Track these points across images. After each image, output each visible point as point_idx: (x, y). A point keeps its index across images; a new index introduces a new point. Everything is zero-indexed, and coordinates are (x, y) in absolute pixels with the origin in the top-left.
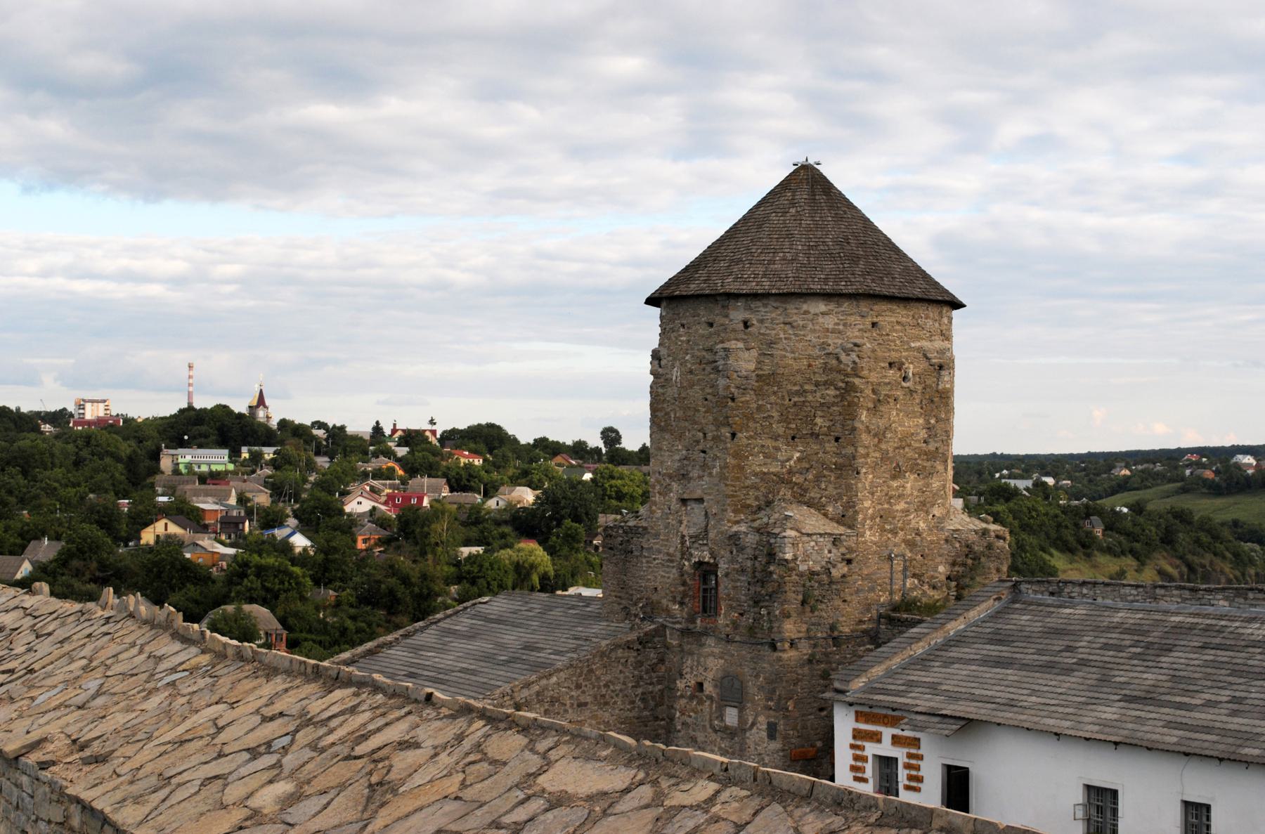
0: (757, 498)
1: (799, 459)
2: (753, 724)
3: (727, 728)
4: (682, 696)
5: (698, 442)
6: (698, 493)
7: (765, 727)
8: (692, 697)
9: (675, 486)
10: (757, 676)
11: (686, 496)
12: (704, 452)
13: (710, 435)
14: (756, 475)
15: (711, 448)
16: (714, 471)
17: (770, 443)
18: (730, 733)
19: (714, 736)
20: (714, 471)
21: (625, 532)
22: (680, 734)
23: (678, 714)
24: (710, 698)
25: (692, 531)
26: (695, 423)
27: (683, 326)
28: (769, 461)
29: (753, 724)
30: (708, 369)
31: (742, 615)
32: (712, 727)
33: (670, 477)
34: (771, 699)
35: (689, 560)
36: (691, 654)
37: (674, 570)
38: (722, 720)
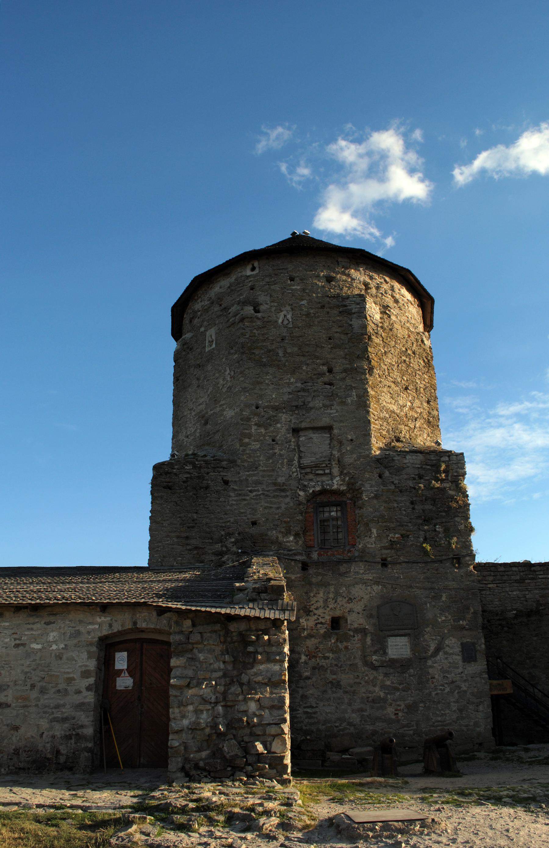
0: (388, 431)
1: (412, 408)
2: (438, 650)
3: (393, 662)
4: (310, 636)
5: (322, 374)
6: (325, 421)
7: (458, 650)
8: (327, 636)
9: (284, 417)
10: (437, 597)
11: (303, 425)
12: (331, 384)
13: (337, 369)
14: (387, 410)
15: (343, 379)
16: (349, 400)
17: (393, 385)
18: (400, 666)
19: (372, 674)
20: (349, 400)
21: (195, 466)
22: (309, 682)
23: (303, 658)
24: (363, 631)
25: (306, 461)
26: (318, 358)
27: (292, 279)
28: (394, 401)
29: (438, 650)
30: (335, 312)
31: (402, 535)
32: (367, 663)
33: (276, 409)
34: (464, 619)
35: (304, 490)
36: (325, 585)
37: (288, 500)
38: (385, 653)
